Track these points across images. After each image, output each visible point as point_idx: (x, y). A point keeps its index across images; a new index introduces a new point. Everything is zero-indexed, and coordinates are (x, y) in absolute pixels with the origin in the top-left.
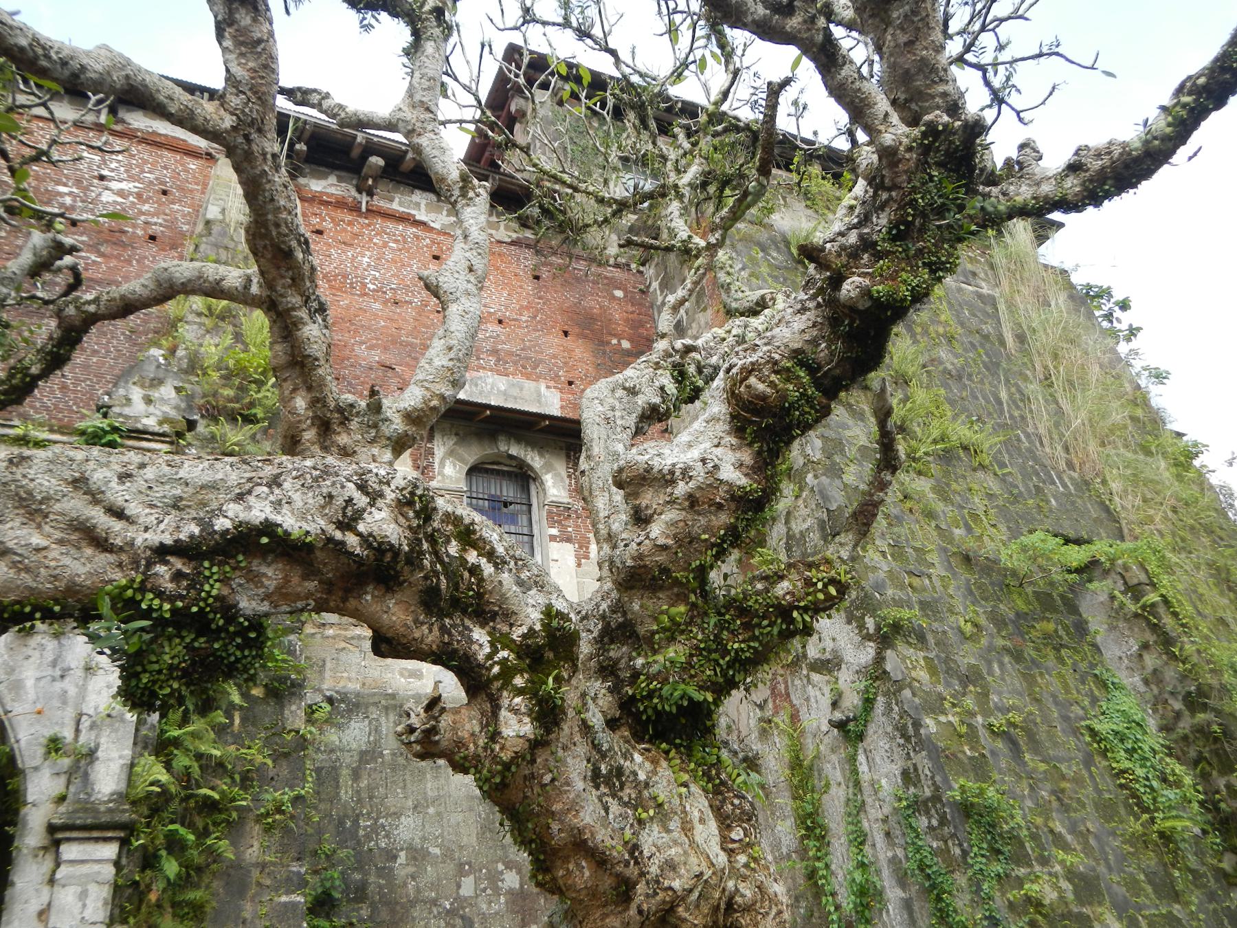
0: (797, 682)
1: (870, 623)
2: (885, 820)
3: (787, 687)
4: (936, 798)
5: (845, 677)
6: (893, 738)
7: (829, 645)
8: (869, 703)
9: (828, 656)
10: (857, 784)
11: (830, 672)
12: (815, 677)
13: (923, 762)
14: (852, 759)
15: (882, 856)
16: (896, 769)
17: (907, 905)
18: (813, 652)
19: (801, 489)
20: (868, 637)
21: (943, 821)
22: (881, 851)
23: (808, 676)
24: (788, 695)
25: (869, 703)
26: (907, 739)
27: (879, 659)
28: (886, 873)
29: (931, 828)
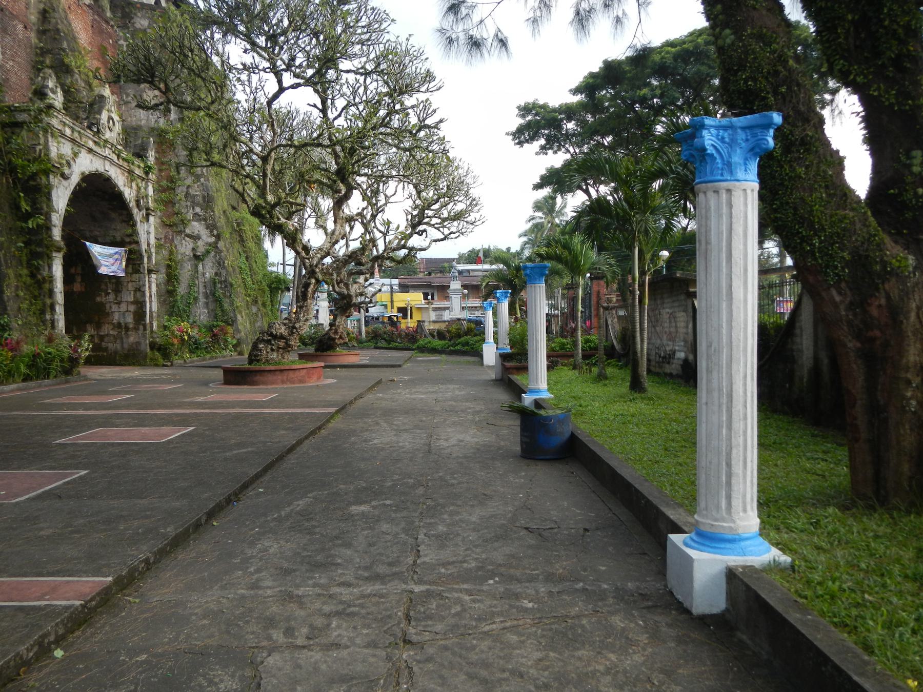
0: (179, 238)
1: (215, 232)
2: (205, 282)
3: (173, 237)
4: (225, 281)
5: (200, 243)
6: (214, 264)
7: (196, 232)
8: (208, 252)
9: (194, 234)
10: (197, 272)
11: (195, 240)
12: (187, 239)
13: (223, 272)
14: (196, 266)
15: (200, 291)
16: (213, 272)
17: (207, 304)
18: (188, 231)
19: (198, 181)
20: (213, 235)
21: (226, 286)
22: (202, 290)
23: (184, 239)
24: (173, 240)
25: (208, 252)
26: (220, 265)
27: (216, 243)
28: (201, 295)
29: (221, 288)
